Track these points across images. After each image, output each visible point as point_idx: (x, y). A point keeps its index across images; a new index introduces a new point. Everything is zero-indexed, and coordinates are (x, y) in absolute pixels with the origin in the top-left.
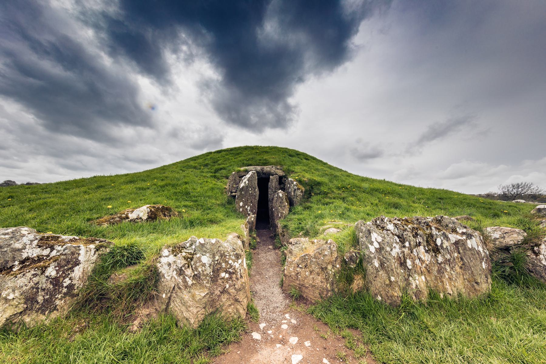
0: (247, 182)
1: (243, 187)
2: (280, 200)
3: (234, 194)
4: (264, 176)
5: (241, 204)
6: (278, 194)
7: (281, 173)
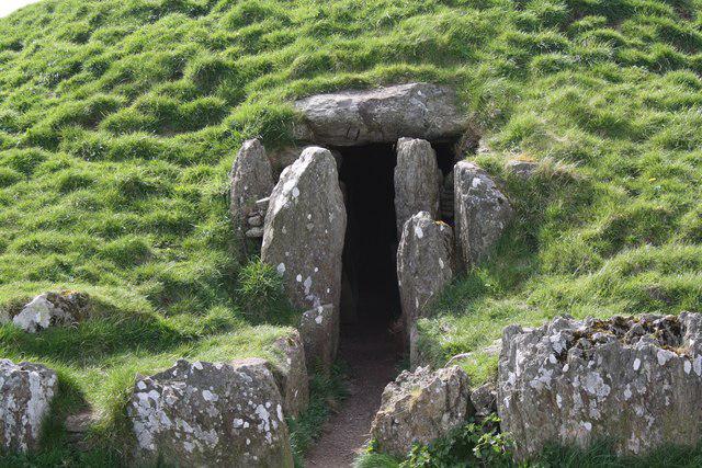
0: (296, 193)
1: (283, 211)
3: (255, 231)
4: (377, 137)
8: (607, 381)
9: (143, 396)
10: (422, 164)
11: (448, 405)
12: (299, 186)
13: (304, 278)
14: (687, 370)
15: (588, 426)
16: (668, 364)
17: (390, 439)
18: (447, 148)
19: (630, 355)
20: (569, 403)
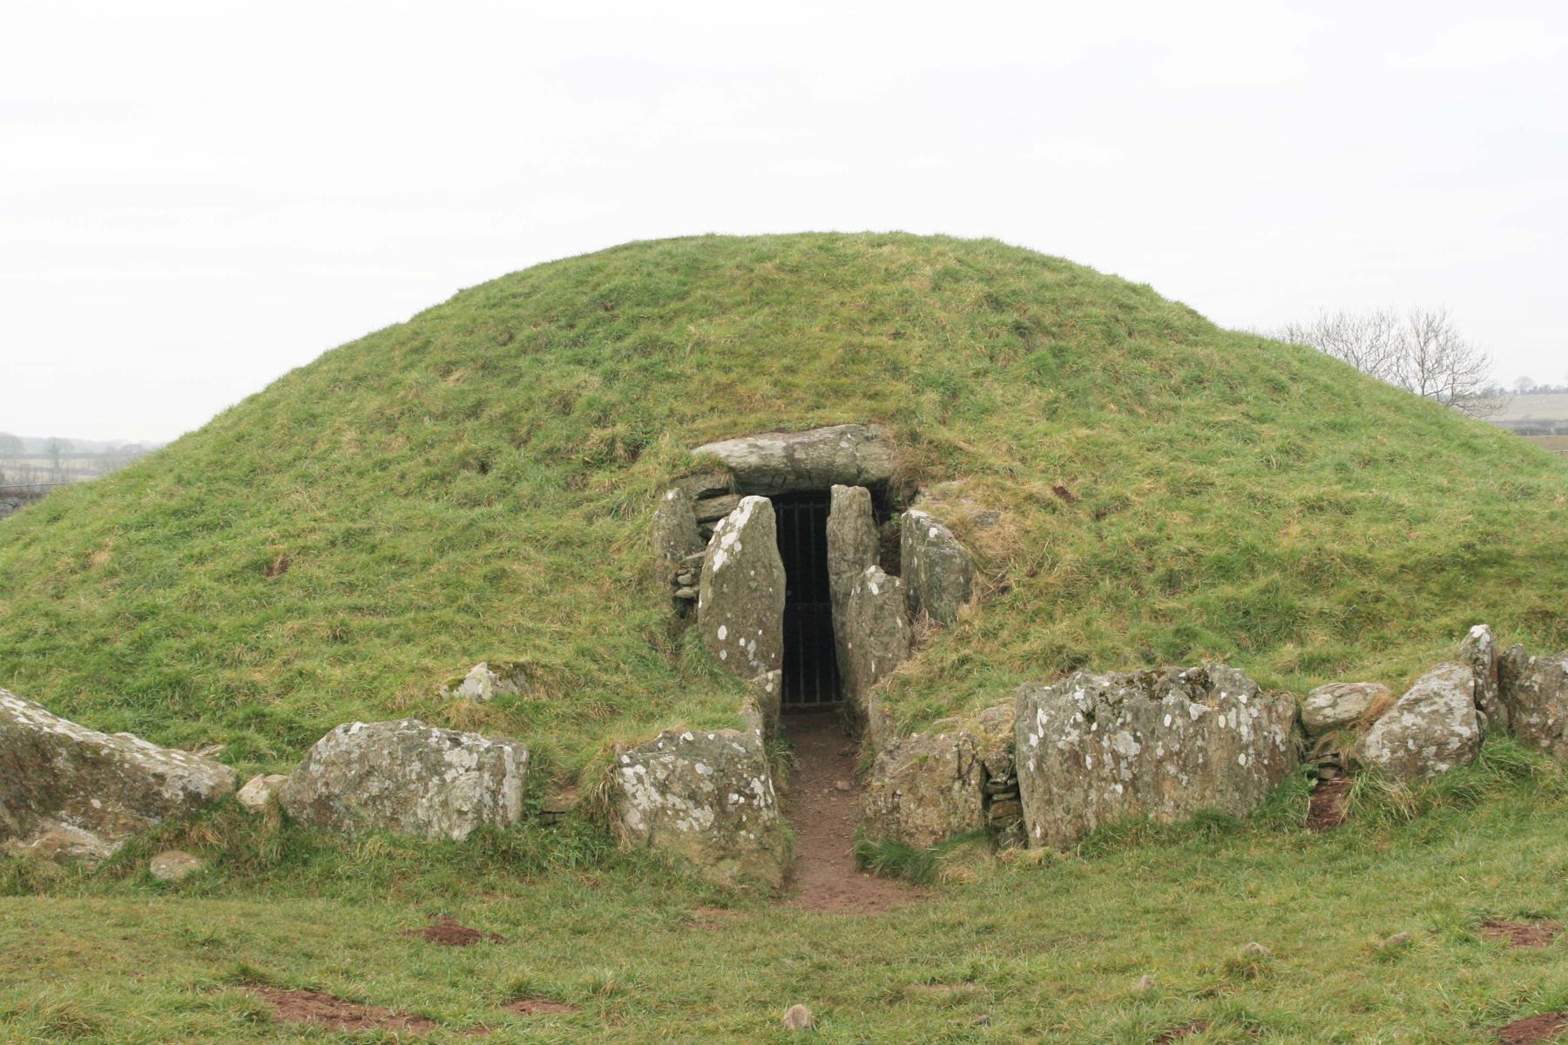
0: (738, 547)
1: (725, 569)
2: (870, 611)
4: (804, 485)
5: (722, 633)
6: (863, 583)
7: (881, 461)
8: (1137, 739)
9: (628, 771)
10: (862, 513)
11: (959, 770)
12: (742, 540)
13: (748, 642)
14: (1222, 725)
15: (1119, 788)
16: (1201, 718)
17: (890, 813)
18: (885, 500)
19: (1160, 711)
20: (1099, 763)
